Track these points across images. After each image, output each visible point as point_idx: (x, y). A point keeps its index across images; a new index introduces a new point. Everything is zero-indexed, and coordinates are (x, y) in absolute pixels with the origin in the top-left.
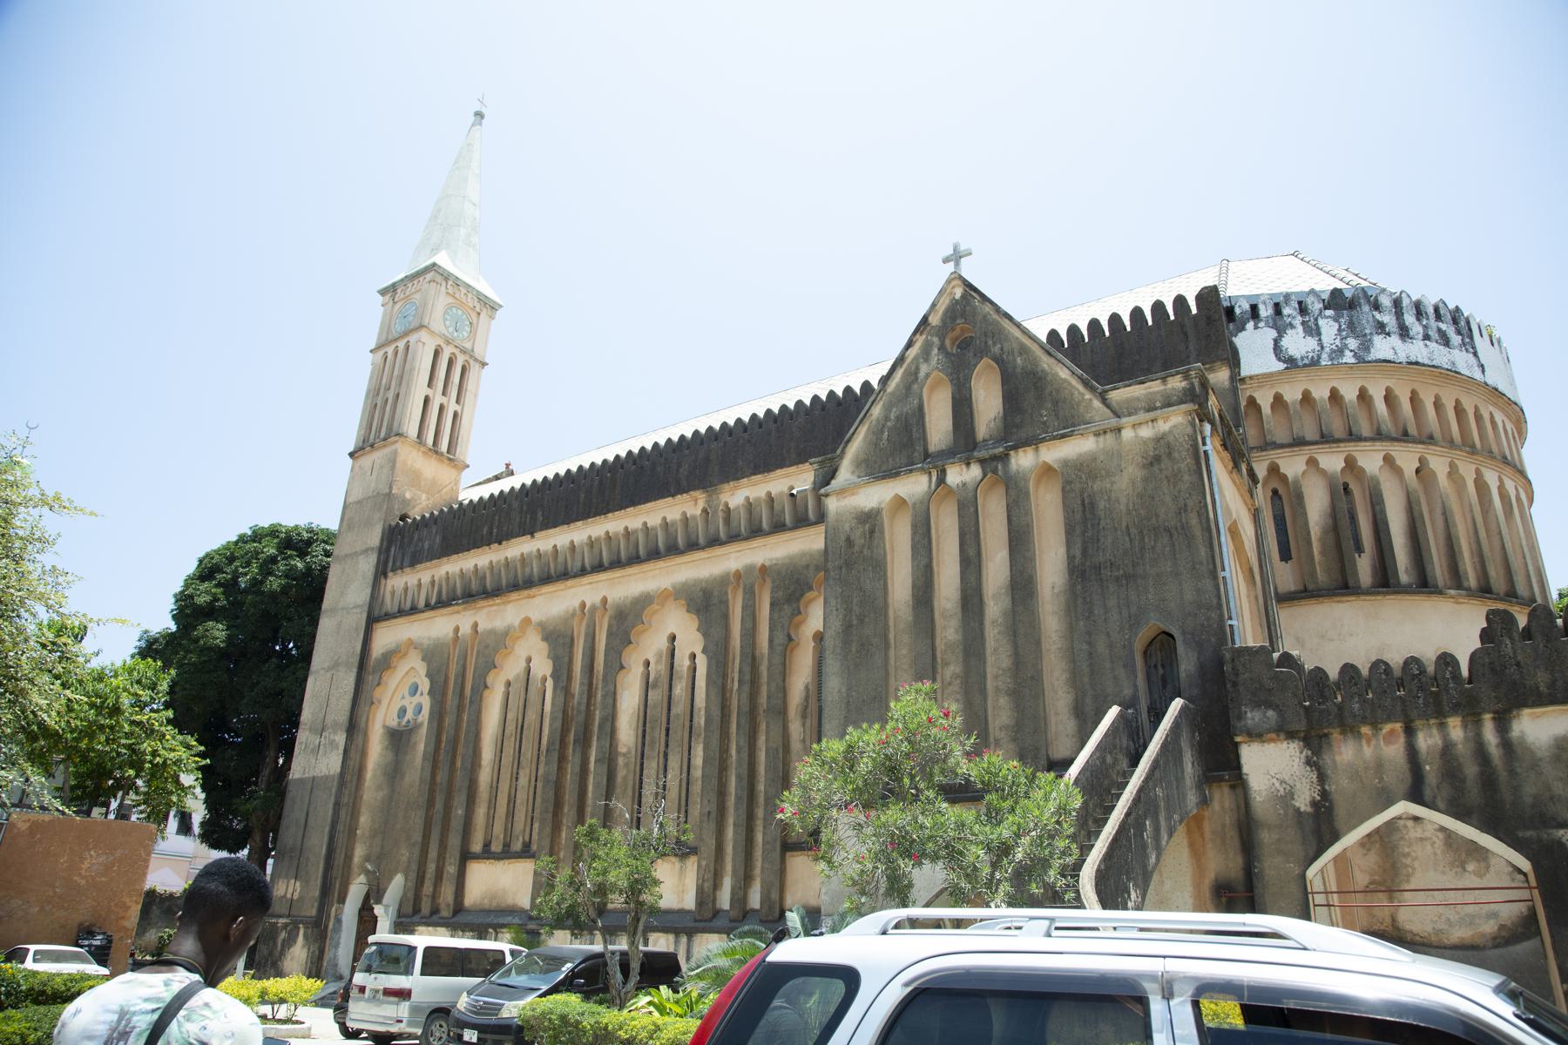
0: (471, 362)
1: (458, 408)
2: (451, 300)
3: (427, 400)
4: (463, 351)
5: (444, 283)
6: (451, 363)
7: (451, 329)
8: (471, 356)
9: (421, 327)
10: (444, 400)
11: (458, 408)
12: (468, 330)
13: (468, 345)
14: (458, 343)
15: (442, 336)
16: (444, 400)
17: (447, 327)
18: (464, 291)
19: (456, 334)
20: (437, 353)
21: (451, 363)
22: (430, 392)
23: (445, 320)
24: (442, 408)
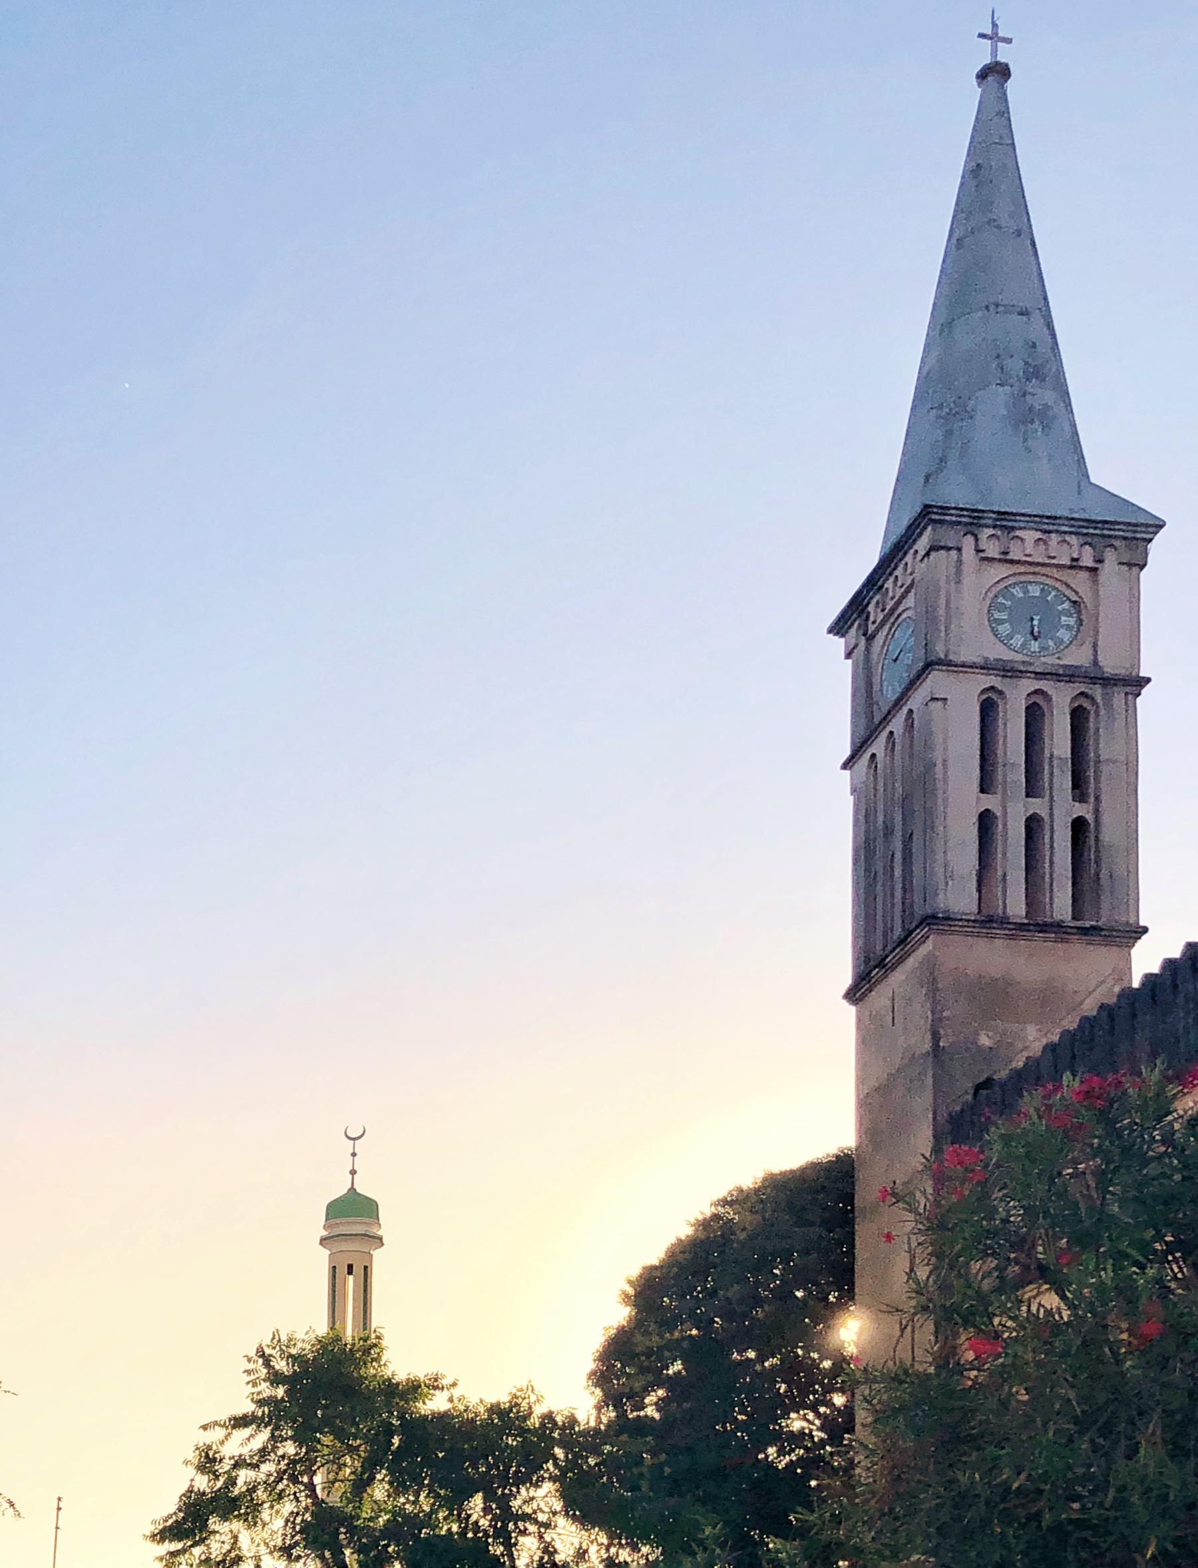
0: (1097, 692)
1: (1083, 810)
2: (1004, 571)
3: (986, 821)
4: (1069, 675)
5: (970, 539)
6: (1035, 715)
7: (1018, 640)
8: (1094, 680)
9: (929, 666)
10: (1038, 806)
11: (1080, 810)
12: (1072, 621)
13: (1078, 657)
14: (1049, 661)
15: (986, 667)
16: (1038, 806)
17: (1005, 641)
18: (1030, 536)
19: (1035, 646)
20: (988, 710)
21: (1035, 715)
22: (990, 802)
23: (994, 624)
24: (1033, 825)
